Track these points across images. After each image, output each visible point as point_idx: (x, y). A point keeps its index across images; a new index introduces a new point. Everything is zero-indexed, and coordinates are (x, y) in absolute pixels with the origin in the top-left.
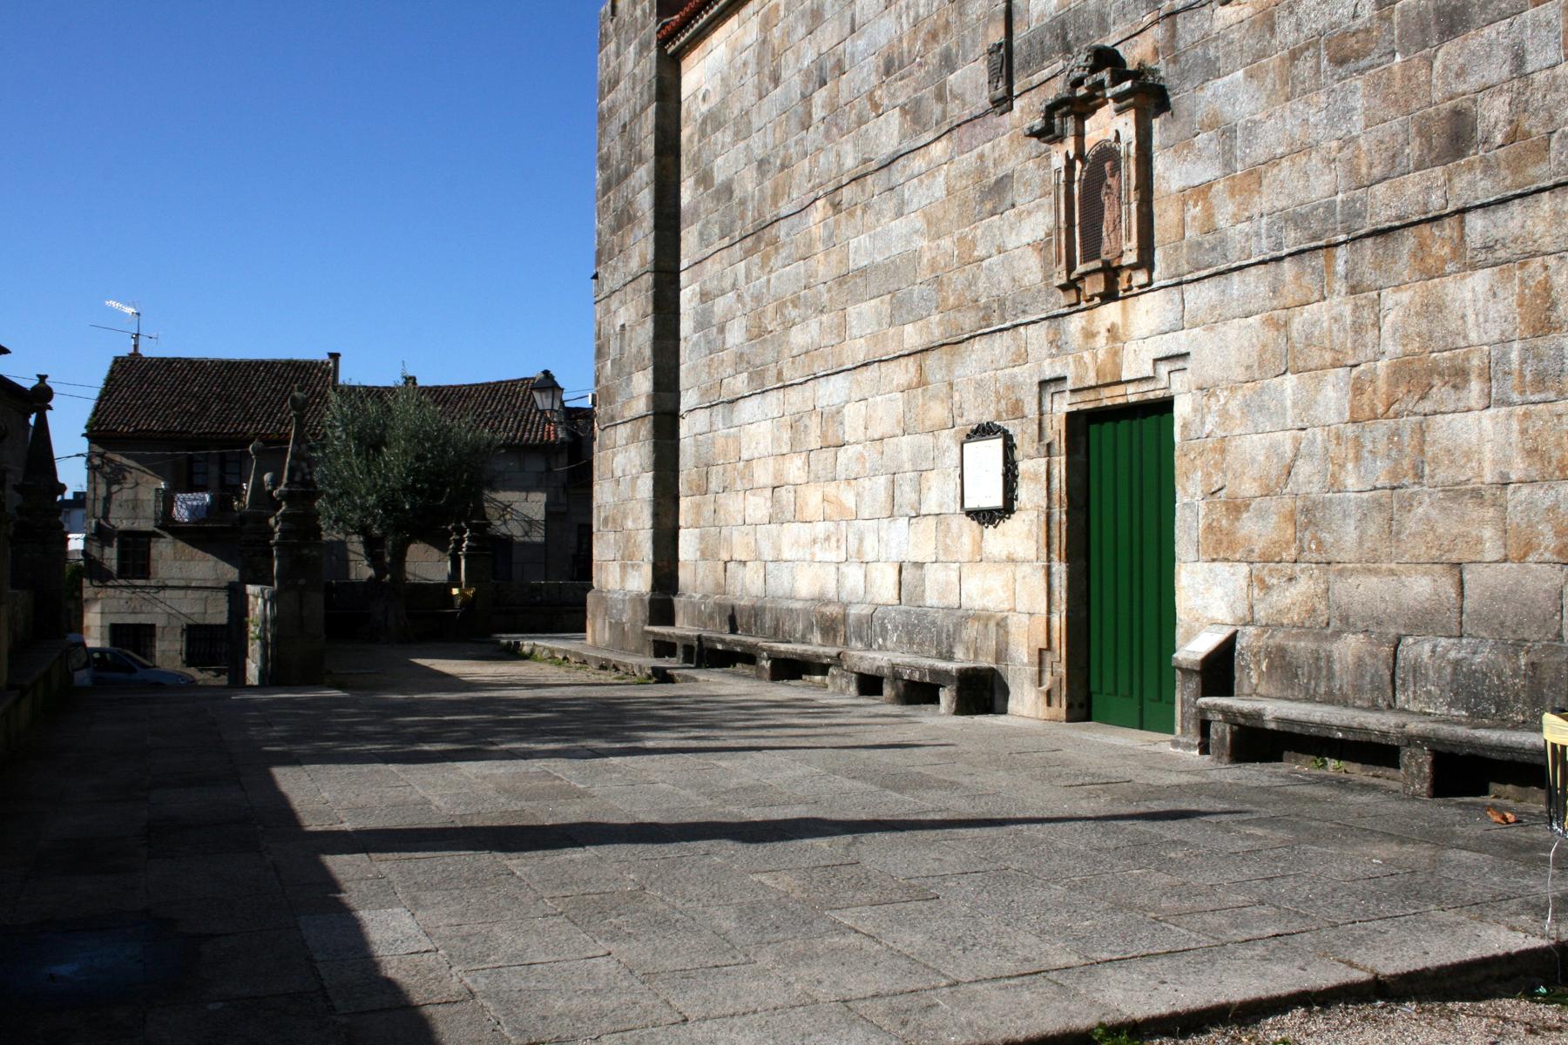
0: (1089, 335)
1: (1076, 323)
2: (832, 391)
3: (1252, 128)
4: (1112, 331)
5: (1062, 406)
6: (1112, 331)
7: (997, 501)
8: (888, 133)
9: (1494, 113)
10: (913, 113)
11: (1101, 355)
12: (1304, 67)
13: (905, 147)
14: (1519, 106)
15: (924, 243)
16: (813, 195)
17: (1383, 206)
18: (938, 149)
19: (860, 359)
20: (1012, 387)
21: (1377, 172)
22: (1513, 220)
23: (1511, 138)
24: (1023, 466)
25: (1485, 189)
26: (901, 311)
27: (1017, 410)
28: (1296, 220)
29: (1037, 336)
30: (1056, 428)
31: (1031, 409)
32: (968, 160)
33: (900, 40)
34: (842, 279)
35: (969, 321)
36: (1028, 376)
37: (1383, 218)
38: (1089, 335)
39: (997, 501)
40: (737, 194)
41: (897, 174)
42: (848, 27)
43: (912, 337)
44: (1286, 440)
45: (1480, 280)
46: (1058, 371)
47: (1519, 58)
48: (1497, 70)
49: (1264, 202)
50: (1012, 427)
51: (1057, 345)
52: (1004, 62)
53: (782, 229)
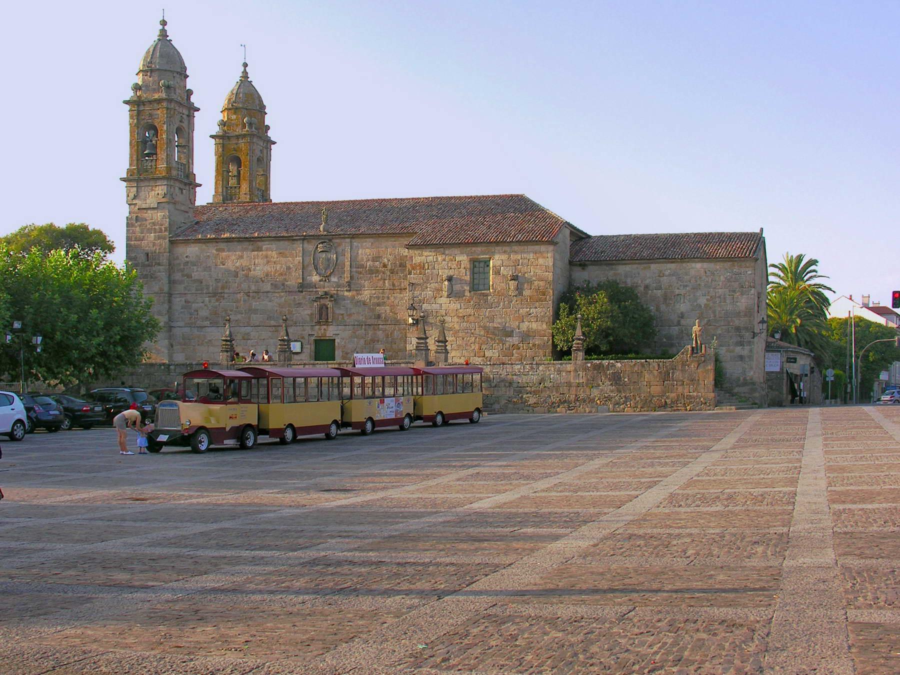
1: (317, 327)
2: (248, 329)
4: (325, 329)
5: (313, 338)
6: (325, 329)
7: (300, 351)
13: (272, 291)
15: (278, 308)
17: (369, 322)
19: (257, 324)
24: (304, 346)
26: (269, 318)
27: (303, 338)
30: (312, 342)
31: (307, 338)
36: (306, 333)
38: (320, 329)
39: (300, 351)
40: (204, 283)
41: (269, 295)
51: (312, 329)
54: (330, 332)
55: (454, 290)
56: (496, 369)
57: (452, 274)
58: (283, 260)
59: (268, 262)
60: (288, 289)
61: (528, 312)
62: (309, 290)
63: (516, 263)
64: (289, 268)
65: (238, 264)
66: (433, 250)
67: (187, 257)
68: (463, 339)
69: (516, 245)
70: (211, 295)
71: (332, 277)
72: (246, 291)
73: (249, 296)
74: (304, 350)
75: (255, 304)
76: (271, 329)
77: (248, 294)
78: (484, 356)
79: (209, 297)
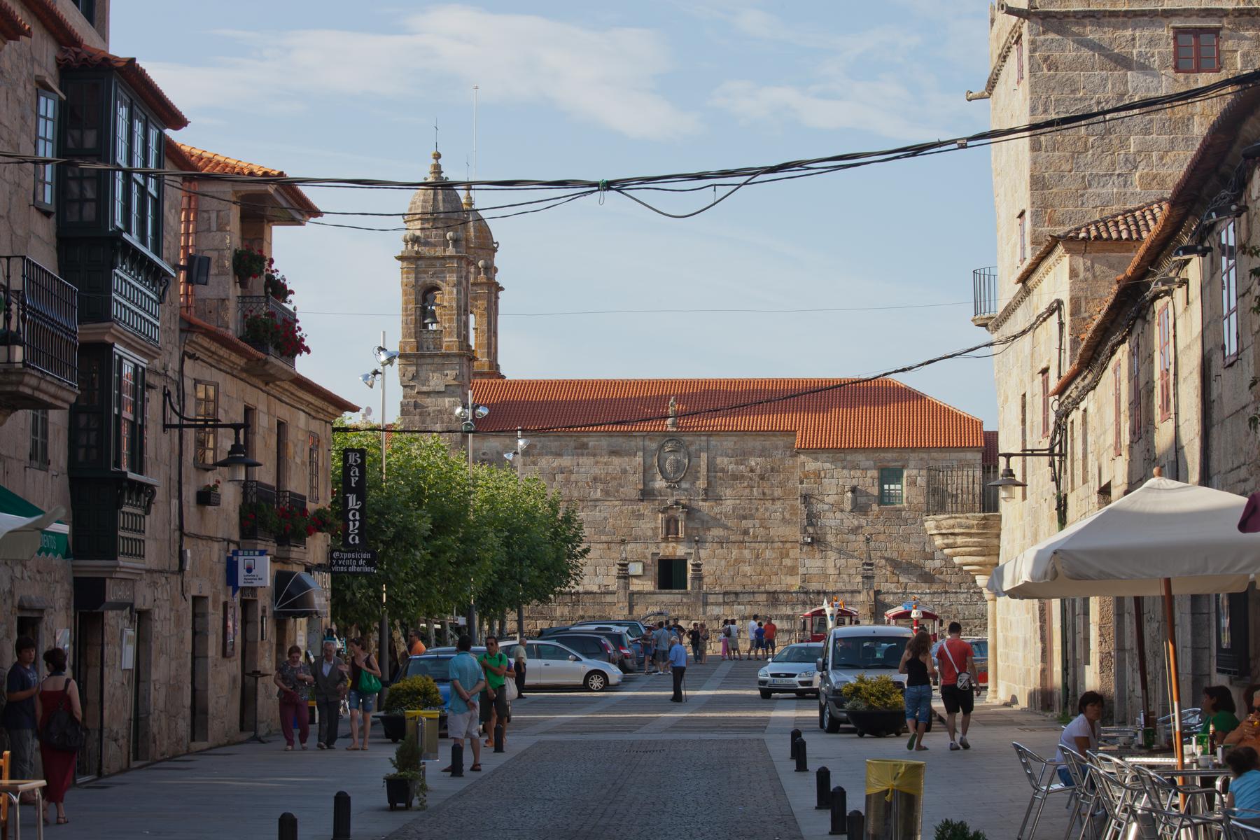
4: (674, 547)
5: (657, 558)
9: (751, 531)
10: (606, 493)
18: (617, 503)
20: (644, 553)
22: (753, 545)
37: (733, 540)
38: (667, 547)
41: (597, 503)
42: (575, 464)
43: (604, 538)
44: (715, 568)
52: (647, 494)
54: (680, 551)
55: (859, 502)
57: (856, 484)
60: (623, 496)
64: (625, 471)
65: (554, 465)
74: (647, 572)
78: (898, 583)
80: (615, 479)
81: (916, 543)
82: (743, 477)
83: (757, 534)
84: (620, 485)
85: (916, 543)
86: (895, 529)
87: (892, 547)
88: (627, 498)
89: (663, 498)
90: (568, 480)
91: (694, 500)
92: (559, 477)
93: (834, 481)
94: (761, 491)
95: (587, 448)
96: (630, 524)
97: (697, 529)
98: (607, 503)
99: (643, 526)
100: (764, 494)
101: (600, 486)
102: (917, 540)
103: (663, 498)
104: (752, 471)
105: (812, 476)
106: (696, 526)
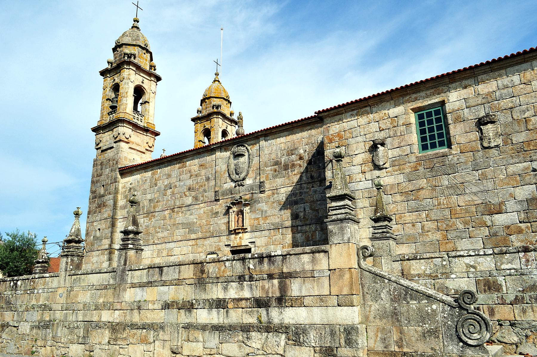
0: (236, 238)
2: (172, 245)
3: (266, 211)
8: (189, 200)
9: (302, 214)
10: (196, 198)
11: (238, 241)
12: (275, 205)
13: (193, 203)
14: (304, 215)
16: (166, 209)
19: (180, 239)
21: (286, 220)
22: (304, 228)
23: (304, 218)
25: (300, 223)
26: (191, 231)
27: (219, 249)
28: (273, 224)
29: (224, 239)
32: (209, 208)
33: (193, 185)
34: (174, 225)
35: (208, 235)
41: (191, 207)
42: (179, 180)
43: (193, 236)
45: (300, 235)
46: (229, 244)
47: (305, 209)
48: (302, 210)
49: (267, 221)
50: (218, 252)
53: (156, 214)
56: (511, 262)
58: (203, 172)
59: (191, 176)
61: (527, 168)
62: (225, 197)
63: (489, 99)
66: (355, 112)
67: (131, 184)
68: (413, 226)
69: (484, 73)
70: (145, 215)
71: (247, 180)
72: (172, 208)
73: (173, 212)
75: (180, 218)
76: (190, 243)
77: (173, 210)
79: (144, 217)
80: (202, 186)
81: (475, 194)
82: (293, 165)
83: (307, 217)
84: (205, 191)
85: (475, 194)
86: (445, 181)
87: (439, 204)
88: (209, 200)
89: (233, 196)
90: (173, 194)
91: (255, 193)
92: (169, 192)
93: (360, 139)
94: (309, 175)
95: (186, 167)
96: (210, 221)
97: (258, 219)
98: (196, 207)
99: (219, 222)
100: (312, 177)
101: (193, 194)
102: (475, 189)
103: (233, 196)
104: (301, 158)
105: (337, 139)
106: (257, 216)
